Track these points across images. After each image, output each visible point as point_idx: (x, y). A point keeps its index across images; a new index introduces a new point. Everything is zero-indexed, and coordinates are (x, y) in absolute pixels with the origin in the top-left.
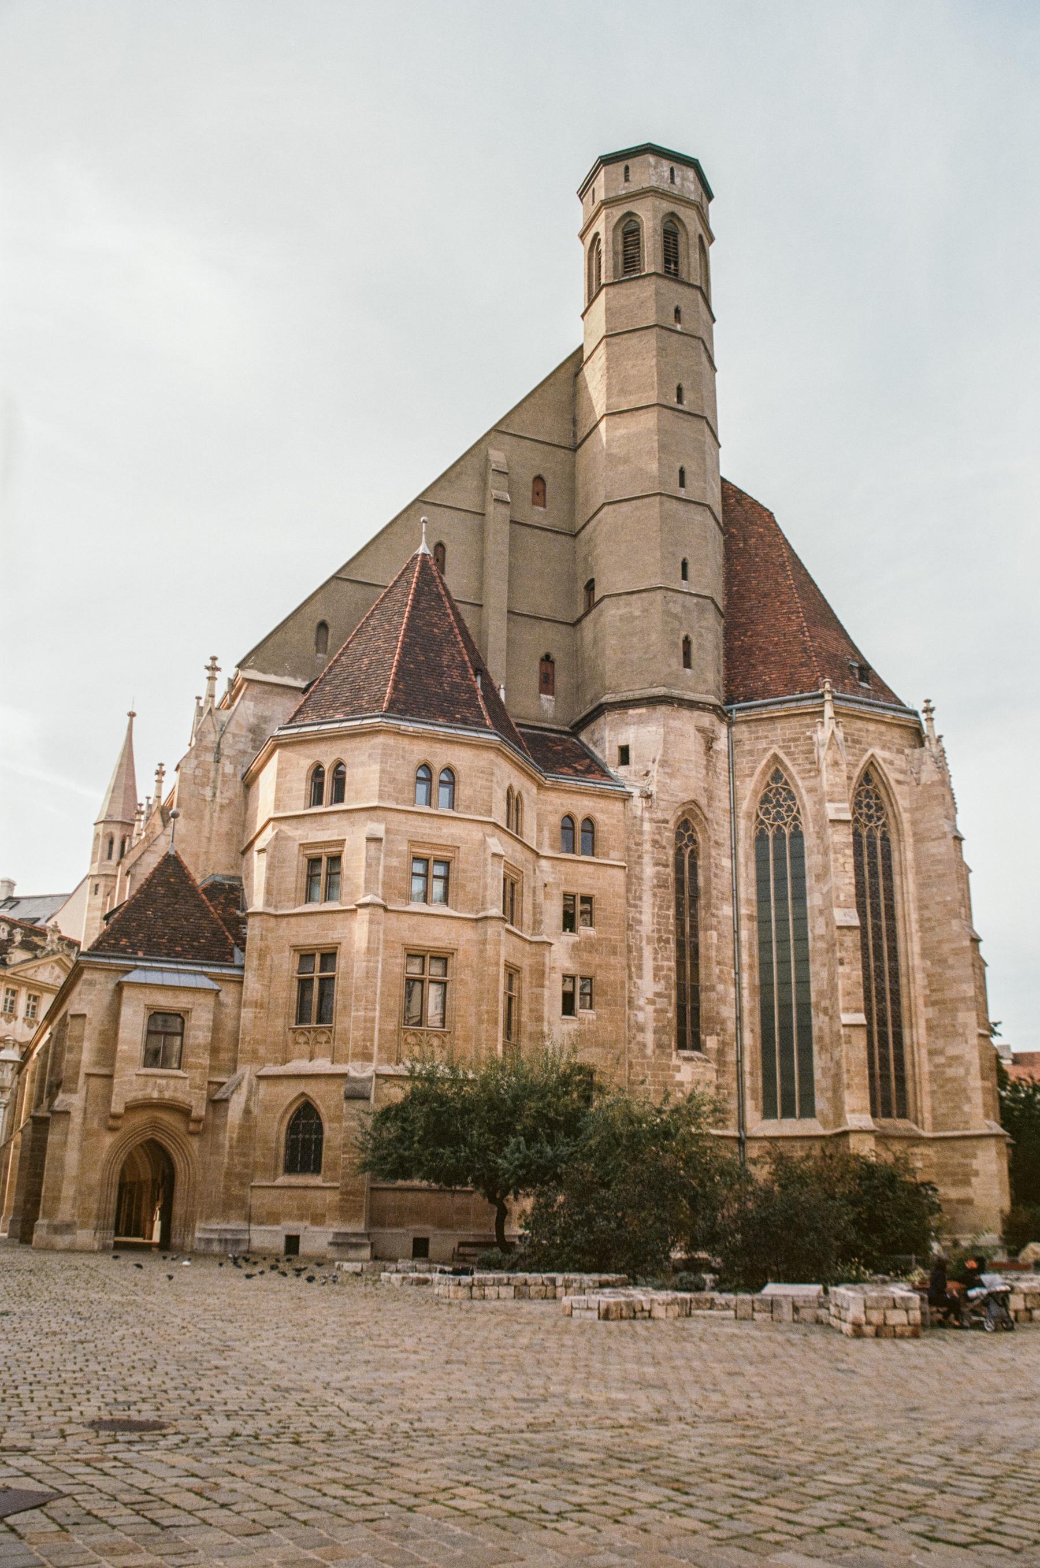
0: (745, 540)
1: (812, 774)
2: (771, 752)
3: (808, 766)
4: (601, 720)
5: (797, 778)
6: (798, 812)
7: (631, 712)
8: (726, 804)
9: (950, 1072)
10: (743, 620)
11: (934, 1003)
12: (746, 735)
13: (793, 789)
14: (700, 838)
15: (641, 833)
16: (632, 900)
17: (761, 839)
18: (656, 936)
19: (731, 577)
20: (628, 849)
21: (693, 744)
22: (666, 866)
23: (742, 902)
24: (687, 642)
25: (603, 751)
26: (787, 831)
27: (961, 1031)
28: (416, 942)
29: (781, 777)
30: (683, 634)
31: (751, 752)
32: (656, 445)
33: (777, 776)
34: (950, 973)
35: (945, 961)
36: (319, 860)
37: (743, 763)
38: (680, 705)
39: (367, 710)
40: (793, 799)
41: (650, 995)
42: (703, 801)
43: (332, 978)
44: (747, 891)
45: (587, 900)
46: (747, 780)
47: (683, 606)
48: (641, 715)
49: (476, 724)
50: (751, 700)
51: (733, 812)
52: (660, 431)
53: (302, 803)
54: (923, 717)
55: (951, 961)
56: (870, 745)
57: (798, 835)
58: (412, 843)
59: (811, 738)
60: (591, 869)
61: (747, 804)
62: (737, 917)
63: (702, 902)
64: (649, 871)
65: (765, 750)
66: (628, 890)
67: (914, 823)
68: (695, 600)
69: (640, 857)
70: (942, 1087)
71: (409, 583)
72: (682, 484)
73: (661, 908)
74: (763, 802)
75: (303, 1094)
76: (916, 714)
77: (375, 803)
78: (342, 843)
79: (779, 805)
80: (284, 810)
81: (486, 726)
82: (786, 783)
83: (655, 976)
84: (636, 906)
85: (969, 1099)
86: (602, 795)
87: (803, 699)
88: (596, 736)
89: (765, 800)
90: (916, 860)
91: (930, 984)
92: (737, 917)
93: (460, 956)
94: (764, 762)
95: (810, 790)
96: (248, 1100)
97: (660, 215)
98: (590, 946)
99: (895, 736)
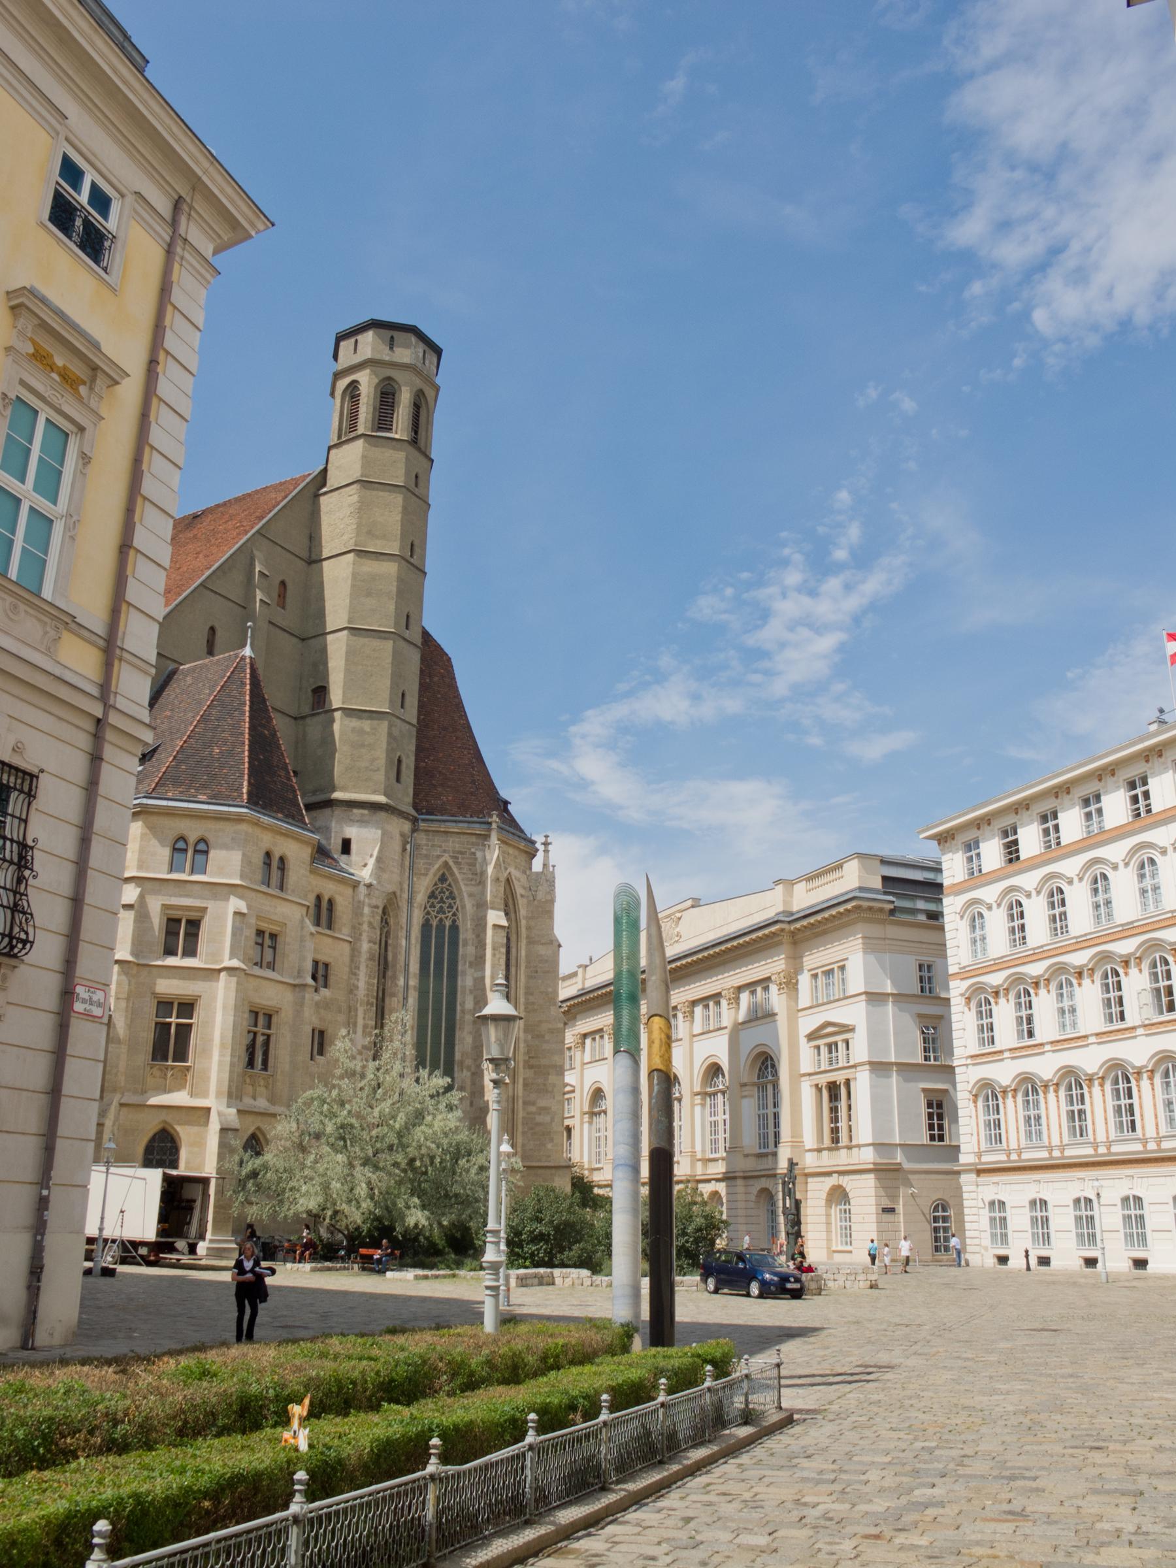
0: (431, 677)
1: (473, 883)
2: (443, 859)
3: (470, 876)
4: (327, 811)
5: (461, 883)
6: (457, 909)
7: (355, 811)
8: (405, 896)
9: (539, 1119)
10: (427, 746)
11: (531, 1067)
12: (424, 842)
13: (456, 892)
14: (392, 921)
15: (362, 914)
16: (353, 972)
17: (426, 926)
18: (366, 999)
19: (423, 708)
20: (354, 927)
21: (396, 845)
22: (375, 943)
23: (411, 975)
24: (400, 761)
25: (328, 839)
26: (448, 923)
27: (550, 1089)
28: (258, 1001)
29: (446, 880)
30: (398, 754)
31: (427, 856)
32: (394, 589)
33: (443, 879)
34: (545, 1046)
35: (543, 1036)
36: (179, 921)
37: (421, 864)
38: (393, 813)
39: (228, 797)
40: (454, 898)
41: (360, 1048)
42: (398, 894)
43: (190, 1025)
44: (414, 967)
45: (326, 965)
46: (422, 877)
47: (401, 731)
48: (362, 815)
49: (299, 821)
50: (431, 814)
51: (410, 901)
52: (400, 580)
53: (166, 867)
54: (541, 848)
55: (547, 1037)
56: (509, 864)
57: (455, 928)
58: (259, 918)
59: (474, 854)
60: (330, 940)
61: (421, 897)
62: (406, 987)
63: (389, 973)
64: (365, 946)
65: (439, 857)
66: (352, 961)
67: (528, 928)
68: (408, 727)
69: (361, 934)
70: (532, 1129)
71: (243, 684)
72: (407, 628)
73: (370, 977)
74: (430, 897)
75: (165, 1122)
76: (533, 843)
77: (238, 882)
78: (204, 910)
79: (442, 901)
80: (147, 870)
81: (306, 824)
82: (450, 885)
83: (364, 1031)
84: (355, 974)
85: (552, 1140)
86: (343, 881)
87: (473, 822)
88: (318, 824)
89: (432, 895)
90: (527, 956)
91: (528, 1052)
92: (406, 987)
93: (283, 1014)
94: (437, 866)
95: (471, 895)
96: (114, 1125)
97: (415, 389)
98: (326, 1005)
99: (522, 859)
